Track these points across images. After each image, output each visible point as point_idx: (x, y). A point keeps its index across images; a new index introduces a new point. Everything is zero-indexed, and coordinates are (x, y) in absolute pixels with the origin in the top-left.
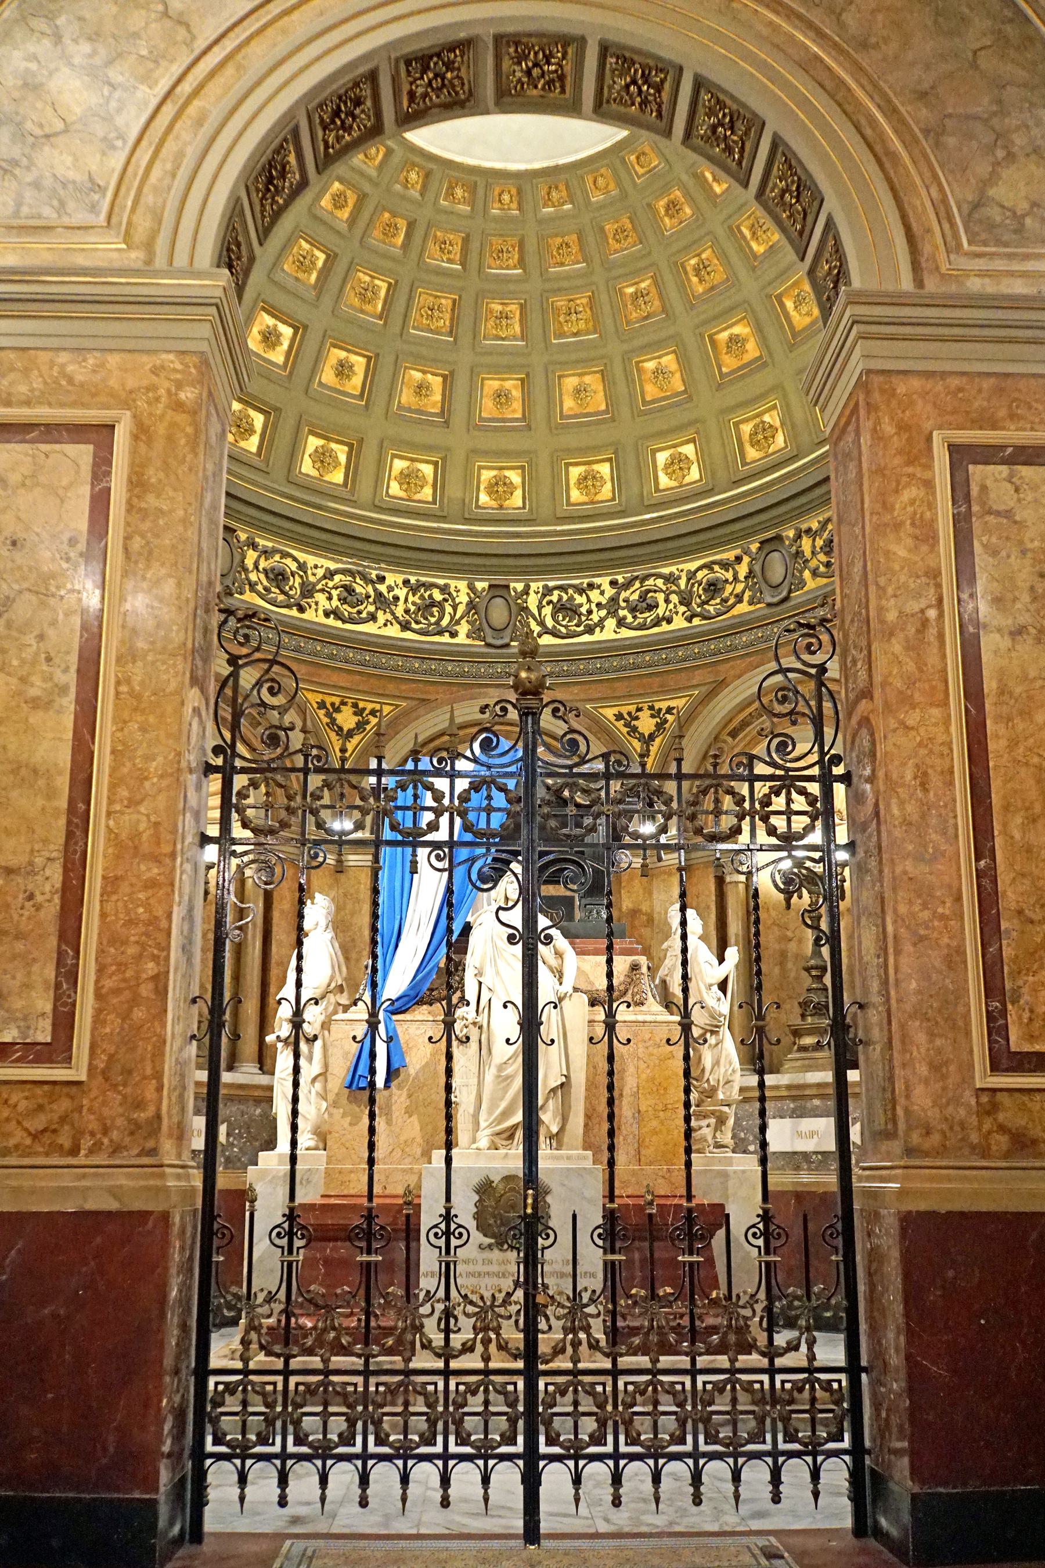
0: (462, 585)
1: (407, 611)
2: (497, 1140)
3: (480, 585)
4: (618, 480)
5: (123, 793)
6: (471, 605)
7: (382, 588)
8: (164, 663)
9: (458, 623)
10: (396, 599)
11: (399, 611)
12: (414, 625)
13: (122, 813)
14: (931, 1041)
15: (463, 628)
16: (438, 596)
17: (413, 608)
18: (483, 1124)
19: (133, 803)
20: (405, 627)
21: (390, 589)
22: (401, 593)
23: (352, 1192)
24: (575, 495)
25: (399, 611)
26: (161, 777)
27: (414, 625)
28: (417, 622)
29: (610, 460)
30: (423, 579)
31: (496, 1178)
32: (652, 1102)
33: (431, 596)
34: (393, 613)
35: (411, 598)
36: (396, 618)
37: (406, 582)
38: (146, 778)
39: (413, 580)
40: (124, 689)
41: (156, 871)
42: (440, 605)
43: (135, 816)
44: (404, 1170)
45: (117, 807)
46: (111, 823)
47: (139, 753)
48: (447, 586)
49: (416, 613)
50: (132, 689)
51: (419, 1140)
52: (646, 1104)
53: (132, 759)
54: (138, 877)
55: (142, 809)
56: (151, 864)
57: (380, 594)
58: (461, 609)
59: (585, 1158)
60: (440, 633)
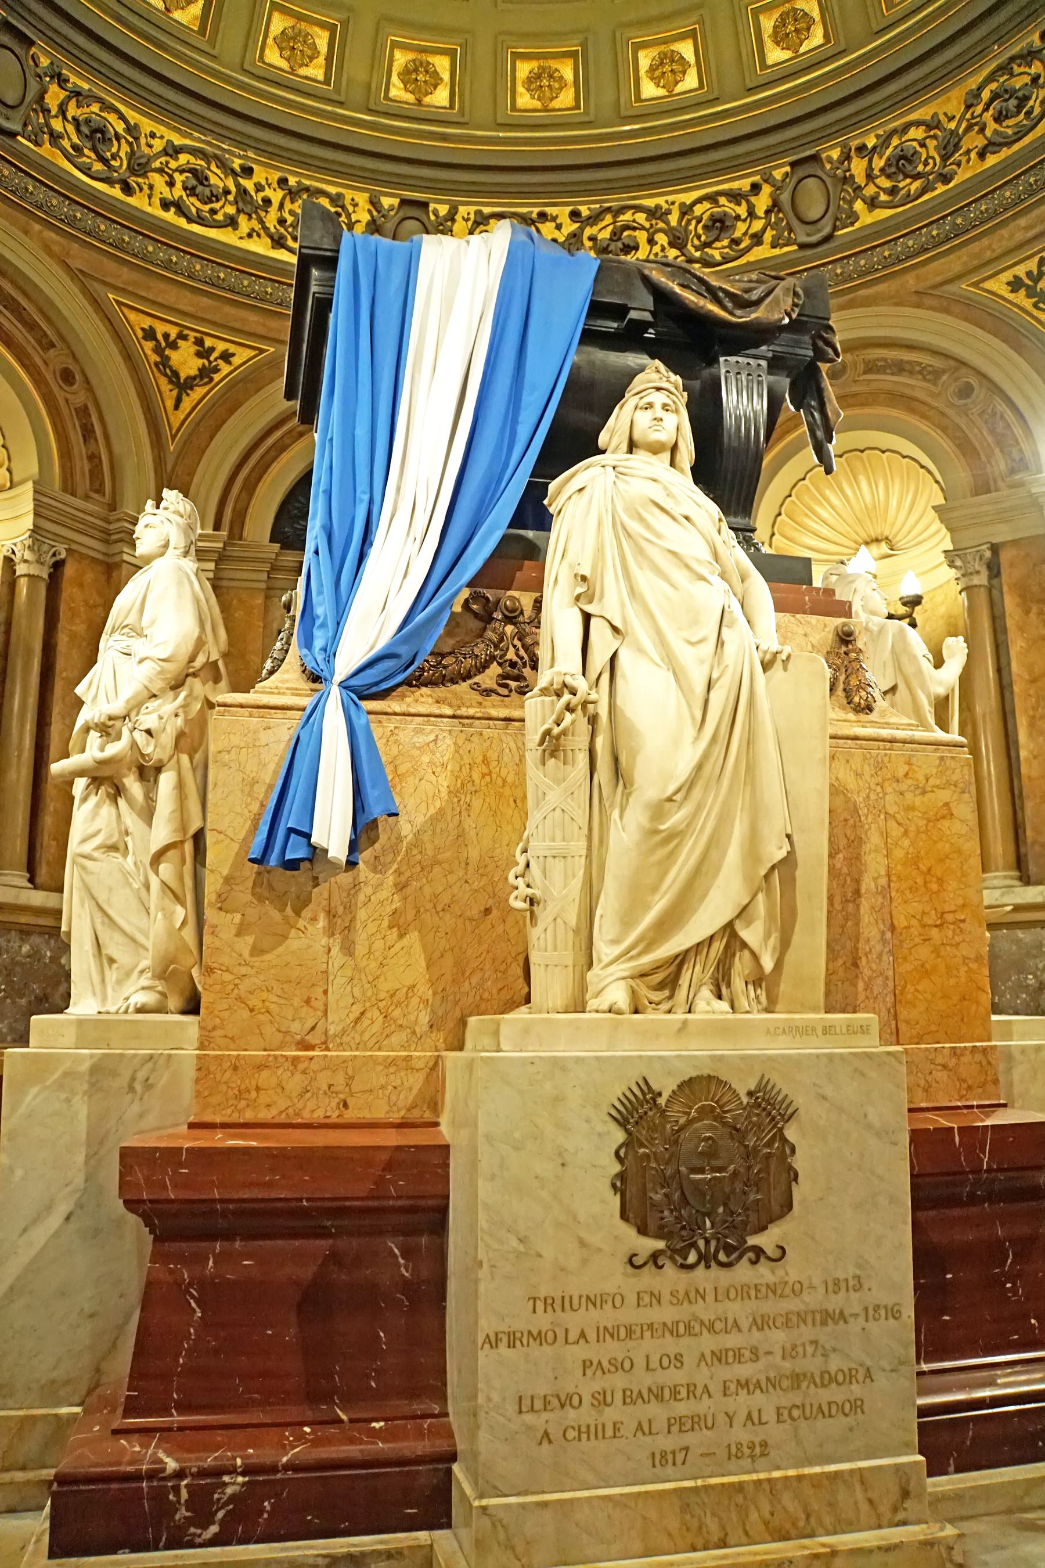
0: (362, 198)
1: (282, 222)
2: (644, 992)
3: (386, 202)
4: (583, 85)
10: (267, 202)
11: (271, 219)
12: (290, 243)
18: (604, 950)
21: (259, 188)
23: (265, 1115)
25: (271, 219)
29: (573, 55)
30: (307, 182)
31: (666, 1086)
32: (916, 907)
34: (261, 222)
36: (265, 229)
37: (283, 182)
39: (292, 181)
44: (393, 1062)
48: (340, 196)
49: (294, 226)
51: (424, 990)
52: (906, 911)
57: (243, 192)
59: (864, 1030)
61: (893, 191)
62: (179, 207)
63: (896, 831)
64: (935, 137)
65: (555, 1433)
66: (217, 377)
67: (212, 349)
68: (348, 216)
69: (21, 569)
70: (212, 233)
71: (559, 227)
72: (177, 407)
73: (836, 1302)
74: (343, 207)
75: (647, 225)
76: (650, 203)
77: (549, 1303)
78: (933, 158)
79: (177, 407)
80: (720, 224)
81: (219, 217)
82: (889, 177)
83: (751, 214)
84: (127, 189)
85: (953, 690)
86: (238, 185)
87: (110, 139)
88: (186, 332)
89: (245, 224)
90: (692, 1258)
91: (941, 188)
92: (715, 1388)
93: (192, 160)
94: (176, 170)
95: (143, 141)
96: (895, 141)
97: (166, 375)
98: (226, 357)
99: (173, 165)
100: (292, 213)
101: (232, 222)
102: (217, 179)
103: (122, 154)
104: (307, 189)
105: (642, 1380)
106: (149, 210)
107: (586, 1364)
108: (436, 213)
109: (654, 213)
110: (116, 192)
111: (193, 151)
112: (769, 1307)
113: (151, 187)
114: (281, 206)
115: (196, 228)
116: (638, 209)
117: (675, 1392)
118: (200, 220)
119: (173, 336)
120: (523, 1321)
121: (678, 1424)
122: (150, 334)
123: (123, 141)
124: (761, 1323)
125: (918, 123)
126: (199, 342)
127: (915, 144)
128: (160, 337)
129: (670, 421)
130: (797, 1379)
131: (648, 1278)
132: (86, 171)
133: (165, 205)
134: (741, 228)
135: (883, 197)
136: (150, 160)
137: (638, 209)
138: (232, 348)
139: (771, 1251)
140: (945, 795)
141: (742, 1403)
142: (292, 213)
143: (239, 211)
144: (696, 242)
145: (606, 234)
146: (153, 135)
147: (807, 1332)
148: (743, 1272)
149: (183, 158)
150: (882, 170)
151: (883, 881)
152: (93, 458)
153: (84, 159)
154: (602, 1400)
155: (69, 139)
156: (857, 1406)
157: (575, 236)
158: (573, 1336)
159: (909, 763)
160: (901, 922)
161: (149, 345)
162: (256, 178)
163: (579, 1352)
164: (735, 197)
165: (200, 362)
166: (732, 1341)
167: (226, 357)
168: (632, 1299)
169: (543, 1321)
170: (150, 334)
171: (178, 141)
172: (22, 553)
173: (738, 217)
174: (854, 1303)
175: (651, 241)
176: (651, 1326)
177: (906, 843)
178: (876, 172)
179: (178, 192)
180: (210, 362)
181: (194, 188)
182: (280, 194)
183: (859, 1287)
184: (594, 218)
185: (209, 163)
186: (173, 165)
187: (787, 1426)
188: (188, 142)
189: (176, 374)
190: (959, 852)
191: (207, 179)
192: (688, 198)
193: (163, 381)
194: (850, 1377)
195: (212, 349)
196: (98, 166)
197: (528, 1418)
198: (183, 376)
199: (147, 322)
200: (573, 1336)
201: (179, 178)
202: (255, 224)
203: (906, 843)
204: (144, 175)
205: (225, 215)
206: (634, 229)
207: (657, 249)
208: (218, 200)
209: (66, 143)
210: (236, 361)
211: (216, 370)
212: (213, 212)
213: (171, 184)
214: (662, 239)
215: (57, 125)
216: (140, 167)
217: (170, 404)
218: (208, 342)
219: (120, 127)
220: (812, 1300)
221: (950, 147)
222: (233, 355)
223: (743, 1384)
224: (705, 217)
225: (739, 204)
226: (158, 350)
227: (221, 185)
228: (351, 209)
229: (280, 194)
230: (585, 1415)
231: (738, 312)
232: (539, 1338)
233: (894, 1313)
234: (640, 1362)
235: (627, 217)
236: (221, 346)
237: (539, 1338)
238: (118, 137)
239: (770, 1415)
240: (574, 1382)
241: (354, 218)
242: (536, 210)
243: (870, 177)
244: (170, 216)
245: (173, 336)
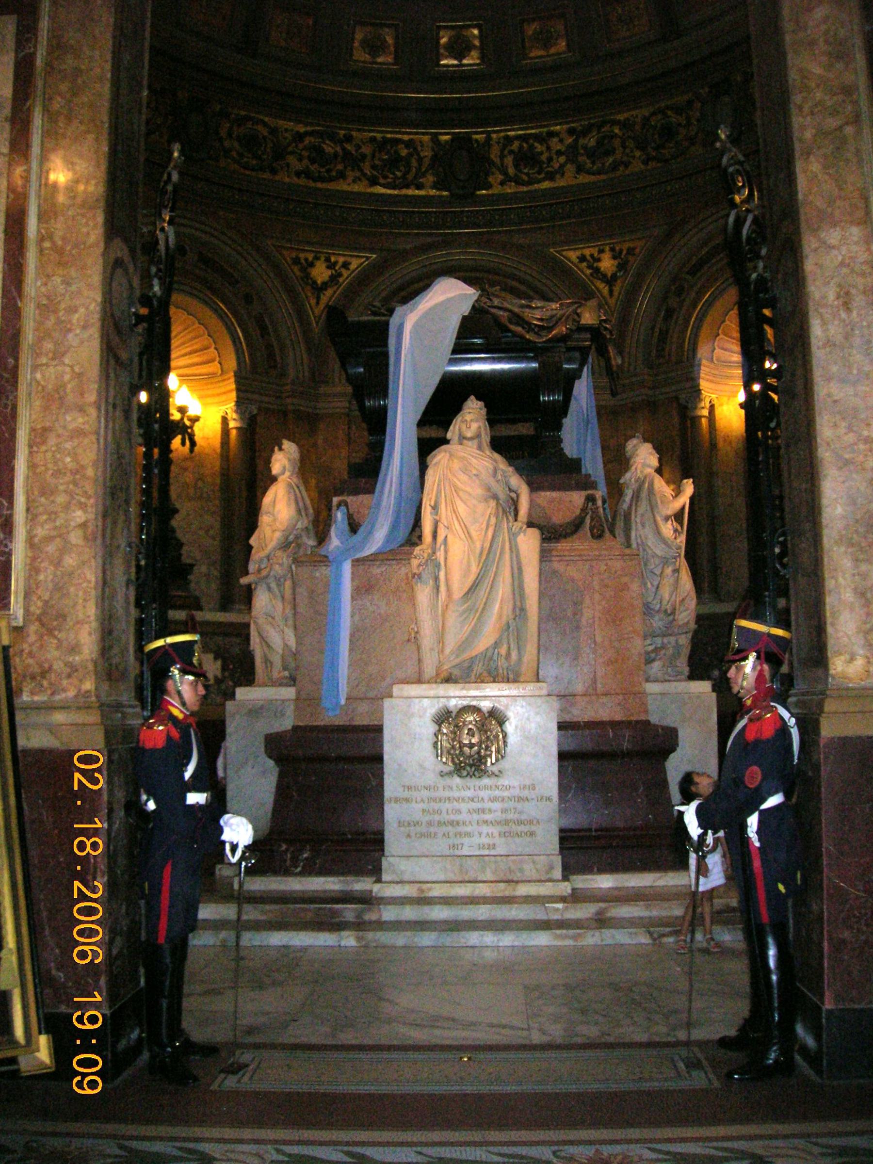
1: (374, 167)
5: (48, 346)
6: (435, 158)
7: (349, 147)
8: (83, 216)
9: (424, 175)
10: (364, 156)
13: (47, 365)
14: (857, 567)
15: (430, 179)
16: (404, 152)
19: (58, 356)
20: (374, 182)
22: (366, 150)
26: (84, 327)
28: (385, 177)
33: (396, 152)
34: (361, 171)
36: (365, 175)
38: (70, 330)
39: (379, 136)
40: (47, 244)
41: (81, 420)
42: (407, 160)
43: (59, 368)
45: (44, 360)
46: (38, 376)
47: (63, 306)
48: (411, 140)
50: (54, 243)
53: (55, 312)
54: (65, 427)
55: (67, 361)
56: (76, 414)
58: (426, 162)
60: (407, 186)
62: (308, 174)
63: (597, 597)
65: (413, 834)
66: (341, 280)
67: (336, 263)
68: (418, 155)
69: (232, 424)
70: (332, 186)
71: (561, 141)
72: (318, 303)
73: (526, 794)
74: (415, 149)
75: (620, 134)
76: (620, 117)
77: (409, 788)
79: (318, 303)
80: (668, 132)
83: (689, 124)
84: (274, 172)
85: (683, 508)
86: (344, 149)
90: (465, 773)
92: (474, 823)
98: (346, 265)
99: (301, 146)
101: (342, 175)
102: (329, 148)
105: (445, 817)
106: (287, 180)
107: (424, 811)
108: (476, 140)
109: (625, 125)
110: (267, 175)
111: (311, 134)
112: (497, 793)
113: (288, 165)
114: (373, 156)
115: (319, 185)
116: (614, 123)
117: (458, 823)
118: (322, 180)
119: (310, 259)
120: (402, 794)
121: (459, 834)
122: (296, 261)
124: (493, 800)
126: (328, 260)
128: (303, 261)
129: (474, 426)
130: (507, 822)
131: (448, 781)
133: (298, 174)
134: (683, 131)
137: (614, 123)
138: (349, 259)
139: (497, 773)
140: (625, 579)
141: (485, 829)
142: (380, 159)
143: (345, 168)
144: (653, 145)
145: (592, 142)
146: (286, 130)
147: (511, 804)
148: (486, 781)
149: (307, 141)
151: (591, 621)
152: (269, 346)
154: (430, 824)
156: (532, 834)
157: (573, 147)
158: (419, 799)
159: (606, 565)
160: (599, 639)
161: (296, 269)
163: (421, 806)
164: (678, 110)
165: (329, 272)
166: (479, 805)
167: (346, 265)
168: (441, 789)
169: (406, 794)
171: (302, 129)
172: (232, 415)
173: (679, 125)
174: (532, 794)
175: (624, 147)
176: (449, 799)
177: (604, 603)
179: (306, 162)
183: (534, 789)
184: (585, 132)
186: (301, 146)
187: (503, 839)
188: (309, 129)
189: (315, 282)
190: (632, 605)
191: (323, 150)
192: (646, 112)
194: (531, 822)
195: (336, 263)
197: (402, 829)
198: (319, 282)
200: (419, 799)
201: (305, 154)
202: (358, 174)
203: (604, 603)
206: (612, 137)
207: (627, 151)
210: (352, 267)
211: (340, 275)
214: (631, 144)
216: (280, 154)
217: (313, 302)
218: (333, 259)
220: (516, 792)
223: (485, 822)
224: (659, 125)
225: (681, 115)
226: (304, 270)
227: (332, 151)
228: (419, 148)
230: (423, 829)
231: (543, 333)
232: (407, 800)
233: (549, 799)
234: (444, 811)
235: (606, 129)
236: (341, 260)
237: (407, 800)
238: (264, 137)
239: (496, 834)
240: (417, 816)
241: (422, 154)
242: (545, 130)
244: (303, 181)
245: (310, 259)
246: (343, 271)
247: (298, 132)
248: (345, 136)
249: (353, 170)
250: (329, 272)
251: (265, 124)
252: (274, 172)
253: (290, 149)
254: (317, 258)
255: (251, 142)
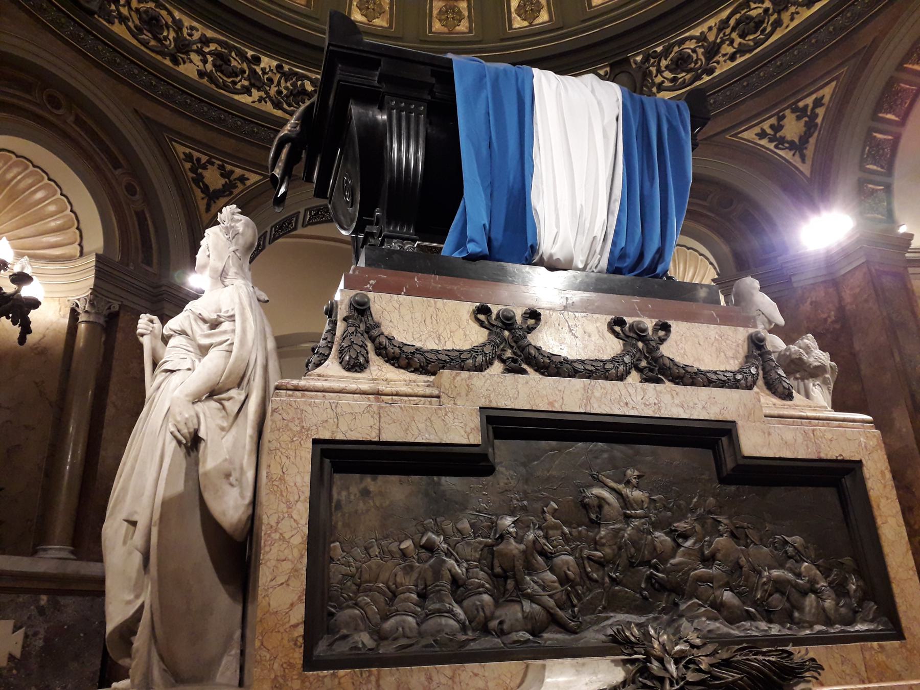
1: (279, 93)
10: (270, 80)
11: (273, 90)
17: (285, 92)
20: (277, 105)
21: (263, 70)
24: (437, 26)
27: (285, 106)
33: (303, 85)
34: (267, 93)
35: (283, 81)
36: (268, 96)
37: (279, 67)
39: (286, 68)
61: (674, 80)
62: (212, 79)
64: (702, 46)
78: (701, 60)
81: (238, 86)
82: (671, 71)
84: (176, 62)
86: (250, 68)
87: (162, 26)
88: (213, 160)
89: (256, 94)
91: (706, 78)
93: (219, 49)
94: (210, 53)
95: (185, 31)
96: (676, 49)
97: (200, 187)
98: (242, 179)
100: (286, 88)
101: (247, 91)
103: (171, 37)
104: (296, 74)
118: (225, 87)
122: (189, 157)
123: (171, 29)
125: (690, 38)
126: (222, 168)
127: (689, 51)
132: (145, 44)
133: (201, 74)
135: (667, 84)
136: (190, 43)
142: (286, 88)
149: (213, 47)
150: (667, 67)
153: (144, 36)
155: (133, 22)
161: (188, 165)
162: (262, 65)
167: (242, 179)
170: (189, 157)
171: (210, 34)
178: (663, 69)
179: (209, 67)
180: (230, 181)
181: (220, 66)
182: (278, 75)
185: (231, 52)
186: (207, 50)
189: (207, 187)
193: (199, 194)
196: (153, 43)
199: (188, 151)
201: (210, 59)
204: (187, 53)
205: (243, 86)
208: (237, 76)
209: (130, 24)
210: (248, 183)
212: (235, 83)
213: (205, 62)
215: (125, 11)
216: (183, 47)
219: (170, 21)
221: (712, 51)
222: (248, 179)
229: (278, 75)
243: (659, 71)
246: (239, 184)
247: (203, 35)
248: (252, 56)
249: (259, 90)
250: (223, 181)
251: (170, 13)
252: (176, 62)
253: (195, 47)
254: (213, 164)
255: (152, 23)
